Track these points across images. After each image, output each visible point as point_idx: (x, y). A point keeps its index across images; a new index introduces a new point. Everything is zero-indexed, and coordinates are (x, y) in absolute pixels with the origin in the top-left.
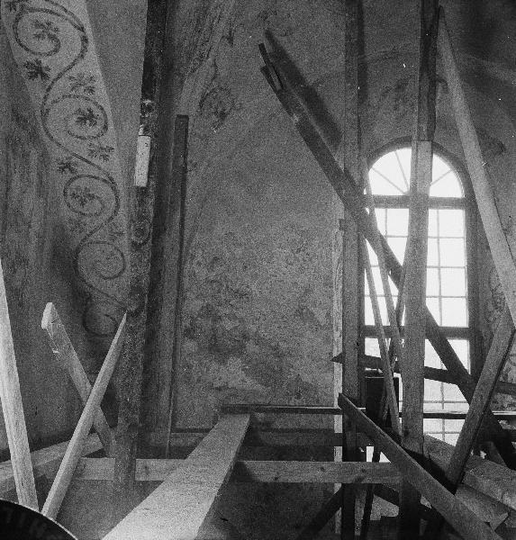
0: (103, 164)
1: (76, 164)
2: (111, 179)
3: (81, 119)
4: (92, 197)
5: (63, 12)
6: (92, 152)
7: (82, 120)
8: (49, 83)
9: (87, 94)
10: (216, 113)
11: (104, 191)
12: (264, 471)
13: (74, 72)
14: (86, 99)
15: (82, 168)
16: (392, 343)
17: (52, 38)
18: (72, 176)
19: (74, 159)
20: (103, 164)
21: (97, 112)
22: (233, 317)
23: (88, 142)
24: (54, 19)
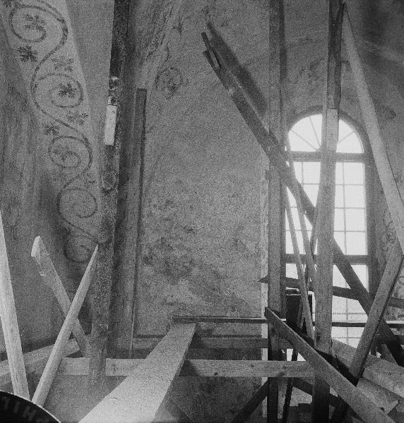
0: (79, 128)
2: (86, 139)
7: (63, 93)
11: (81, 148)
12: (207, 368)
13: (57, 54)
16: (307, 269)
17: (40, 28)
19: (57, 124)
20: (79, 128)
22: (180, 247)
24: (42, 15)
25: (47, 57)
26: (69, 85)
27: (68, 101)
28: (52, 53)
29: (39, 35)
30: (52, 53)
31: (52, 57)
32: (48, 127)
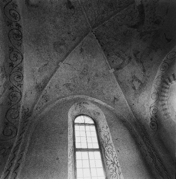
7: (18, 77)
13: (19, 66)
15: (15, 89)
25: (16, 66)
27: (18, 80)
29: (16, 59)
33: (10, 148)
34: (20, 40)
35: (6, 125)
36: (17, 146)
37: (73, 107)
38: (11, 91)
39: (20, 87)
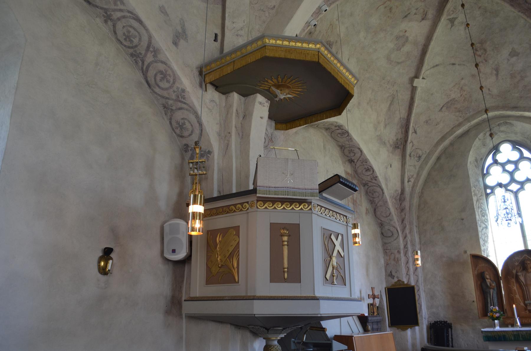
0: (375, 182)
1: (368, 183)
2: (379, 185)
3: (366, 170)
4: (375, 192)
5: (354, 146)
6: (371, 179)
7: (367, 171)
8: (355, 163)
9: (365, 164)
10: (417, 157)
13: (360, 159)
14: (366, 165)
15: (370, 184)
17: (353, 152)
18: (368, 187)
19: (367, 182)
20: (375, 182)
21: (369, 168)
23: (369, 176)
25: (358, 160)
26: (368, 168)
27: (369, 173)
28: (359, 158)
29: (353, 154)
30: (359, 158)
31: (359, 160)
32: (364, 184)
33: (399, 252)
34: (348, 136)
35: (382, 225)
36: (405, 247)
37: (477, 143)
38: (366, 187)
39: (376, 180)
